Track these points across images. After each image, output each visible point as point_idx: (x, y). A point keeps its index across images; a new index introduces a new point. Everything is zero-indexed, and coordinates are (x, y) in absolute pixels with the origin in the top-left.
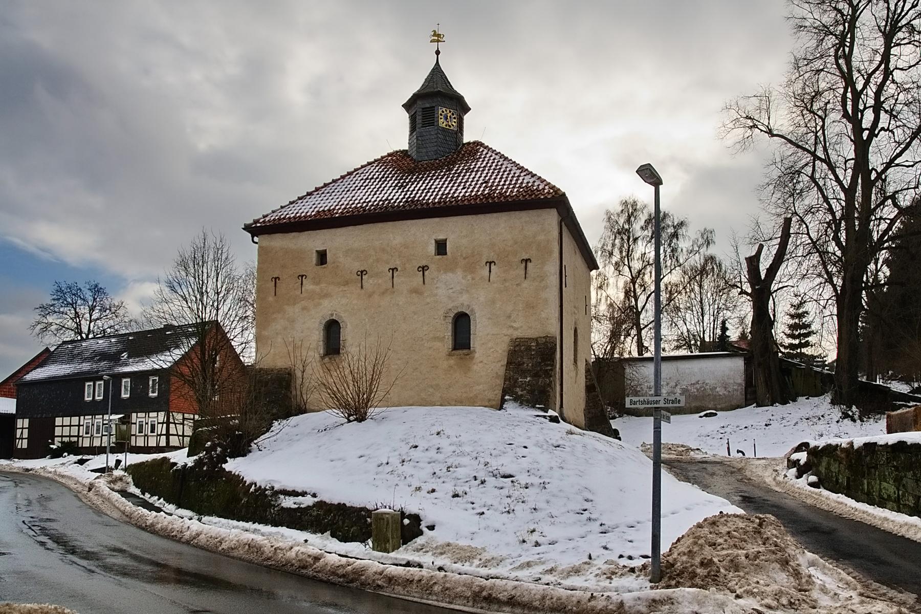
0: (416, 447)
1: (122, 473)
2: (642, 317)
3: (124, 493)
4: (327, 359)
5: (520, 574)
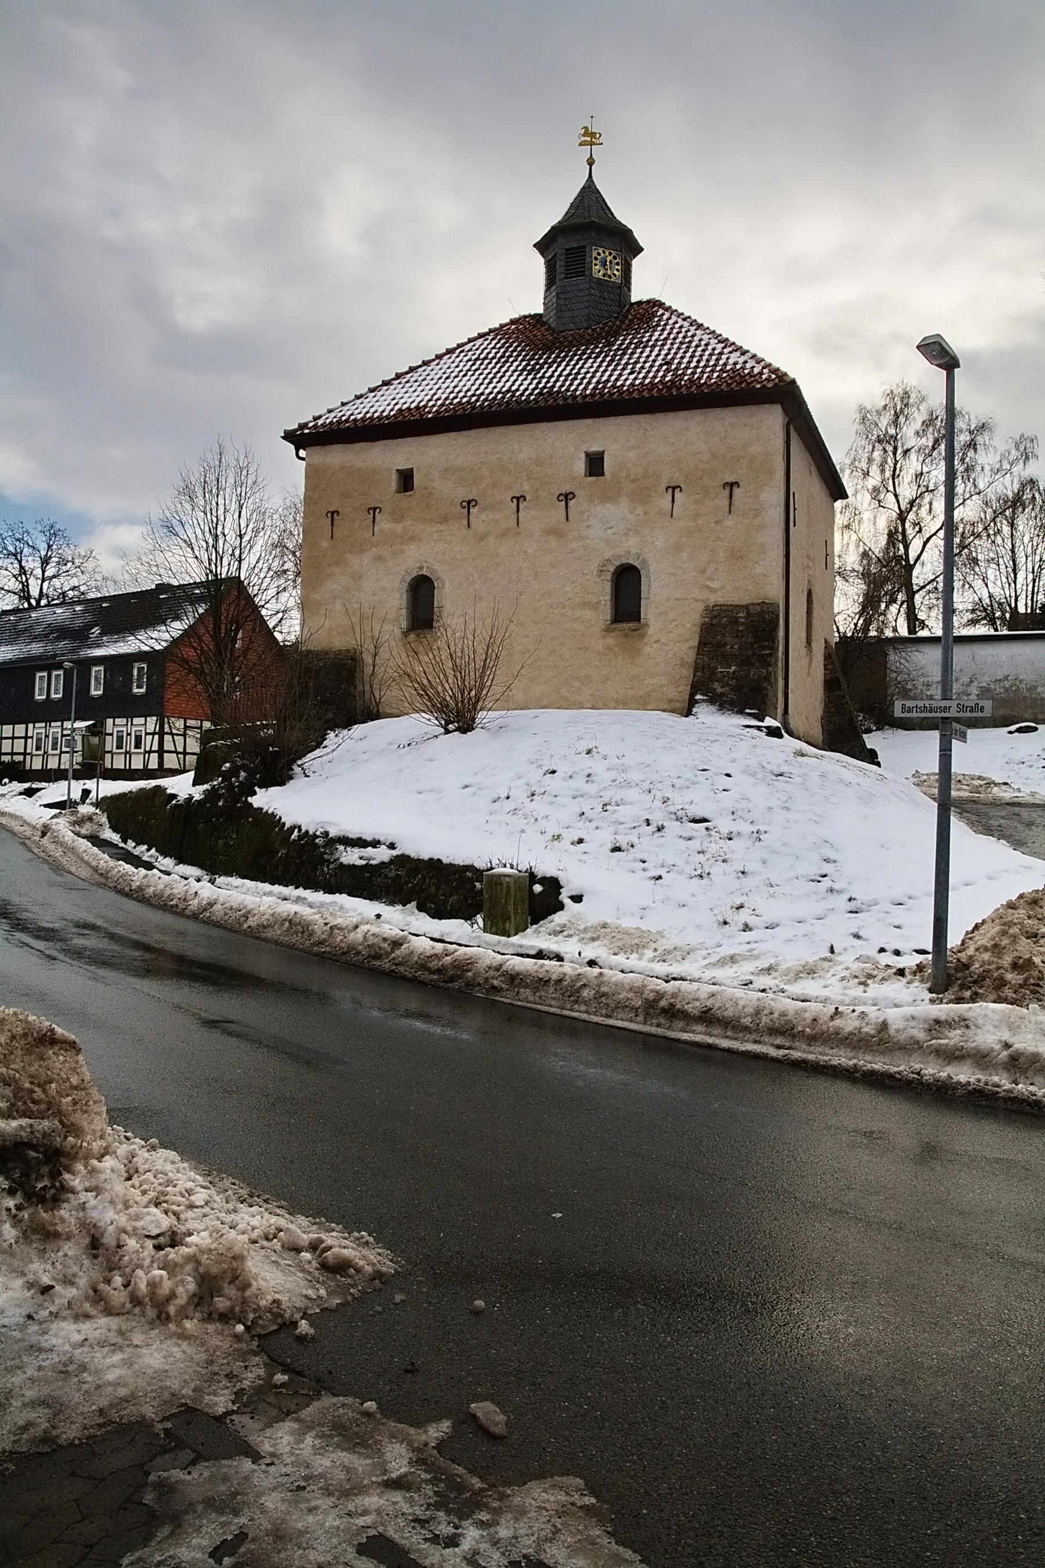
0: (554, 772)
1: (92, 809)
2: (915, 573)
3: (96, 840)
4: (412, 637)
5: (719, 974)
